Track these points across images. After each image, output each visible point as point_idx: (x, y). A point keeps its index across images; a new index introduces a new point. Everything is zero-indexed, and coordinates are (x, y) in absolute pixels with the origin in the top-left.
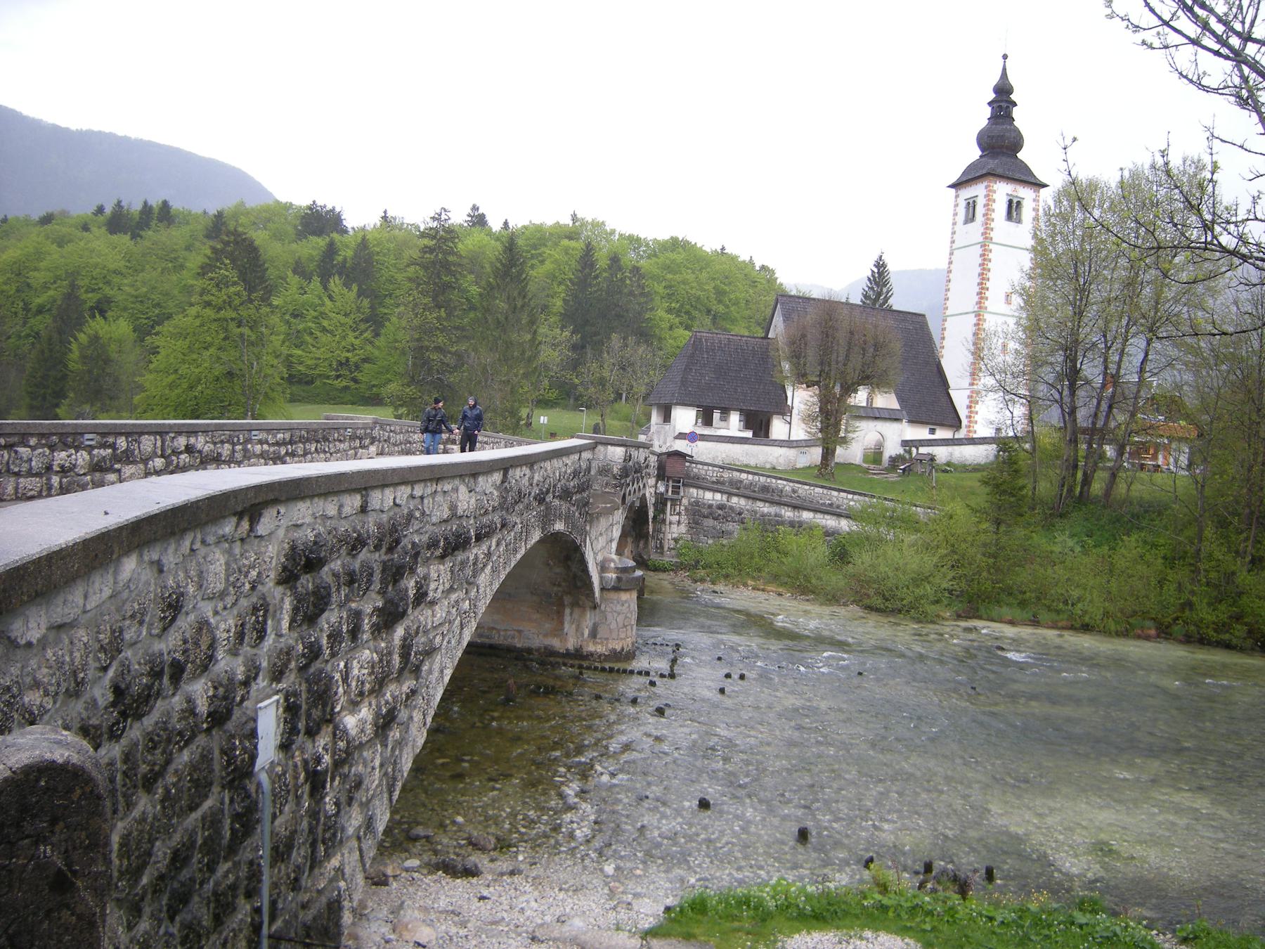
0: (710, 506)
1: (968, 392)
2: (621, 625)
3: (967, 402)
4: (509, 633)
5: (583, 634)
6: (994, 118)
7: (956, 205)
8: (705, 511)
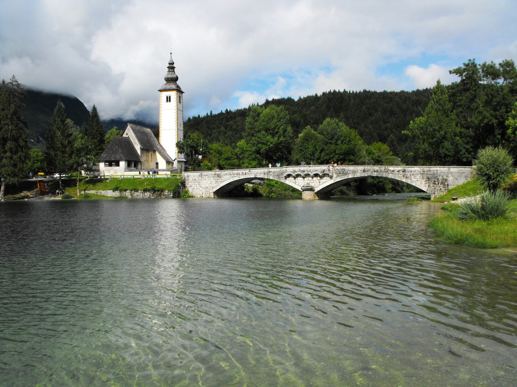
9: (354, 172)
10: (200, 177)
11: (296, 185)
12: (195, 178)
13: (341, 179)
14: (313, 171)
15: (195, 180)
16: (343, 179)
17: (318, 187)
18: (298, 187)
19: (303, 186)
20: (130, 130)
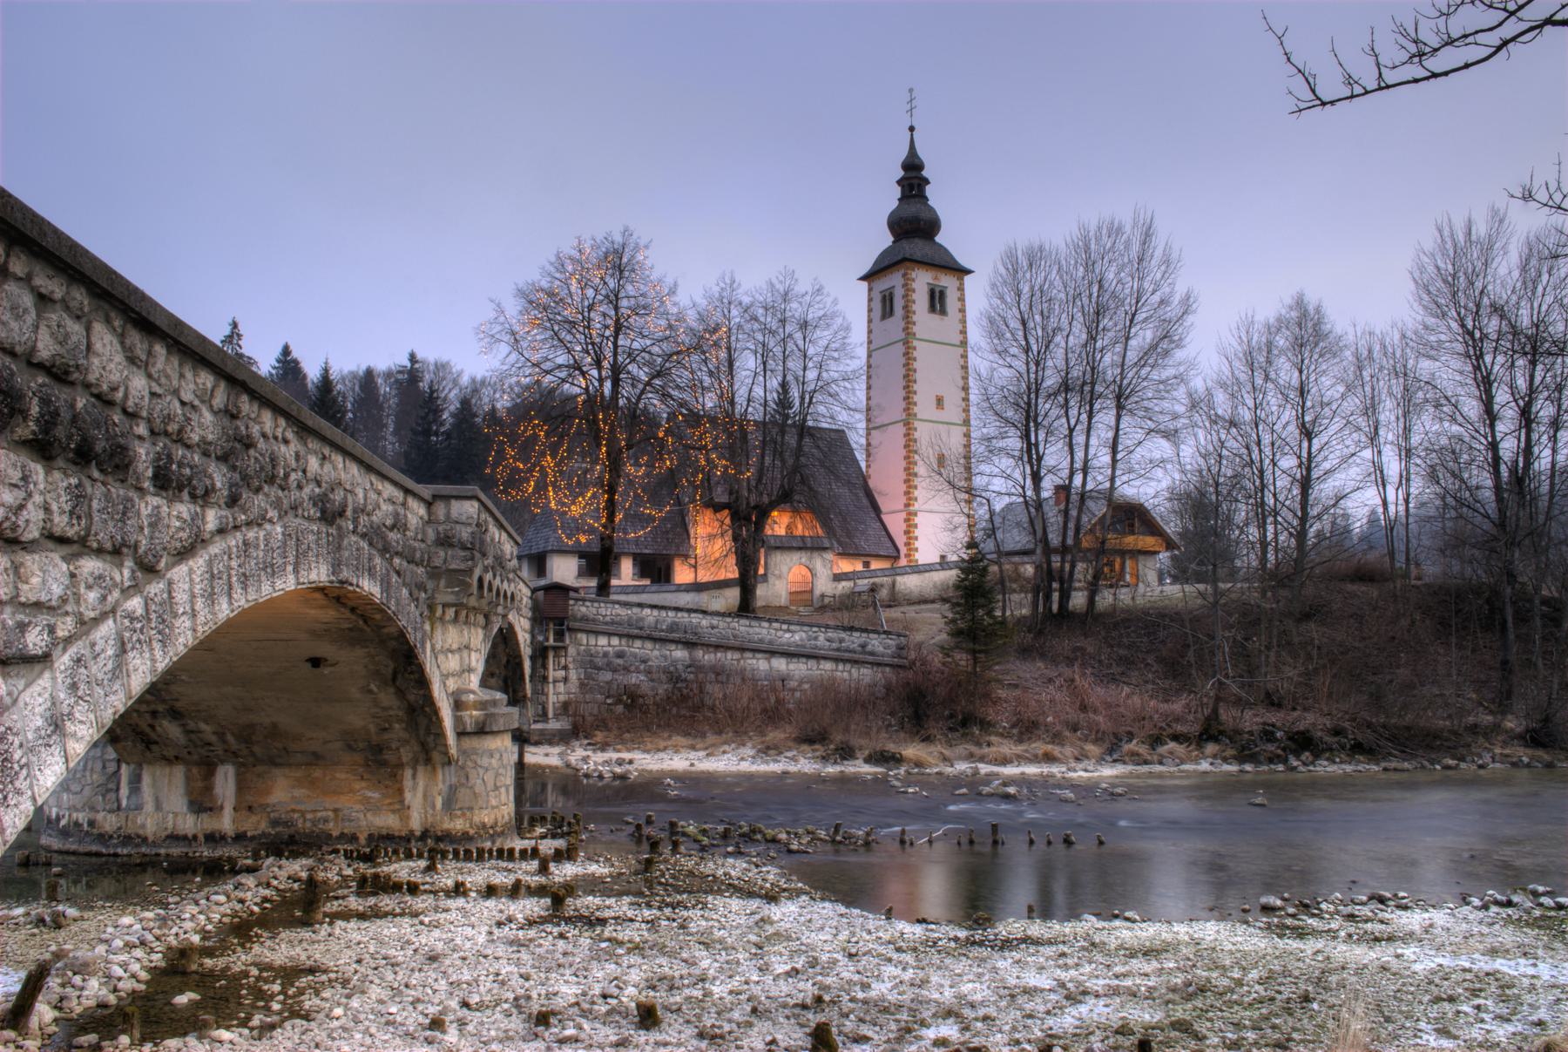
0: (606, 655)
1: (903, 515)
2: (490, 785)
3: (904, 526)
4: (319, 815)
5: (434, 807)
7: (870, 300)
8: (600, 662)
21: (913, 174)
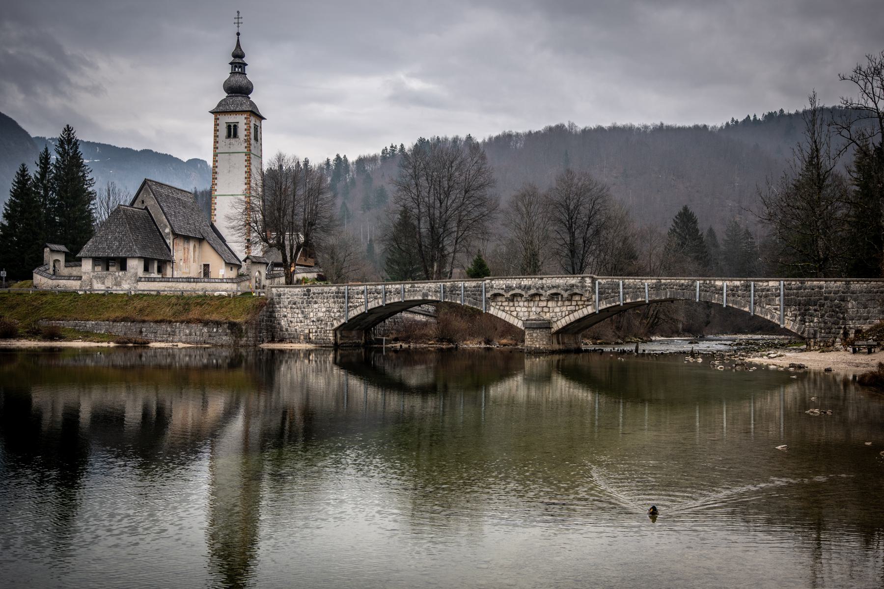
6: (233, 73)
7: (216, 125)
9: (638, 290)
10: (305, 297)
11: (512, 317)
12: (295, 298)
13: (608, 305)
14: (550, 288)
15: (295, 304)
16: (614, 304)
17: (559, 323)
18: (516, 320)
19: (527, 320)
20: (149, 195)
21: (237, 60)
